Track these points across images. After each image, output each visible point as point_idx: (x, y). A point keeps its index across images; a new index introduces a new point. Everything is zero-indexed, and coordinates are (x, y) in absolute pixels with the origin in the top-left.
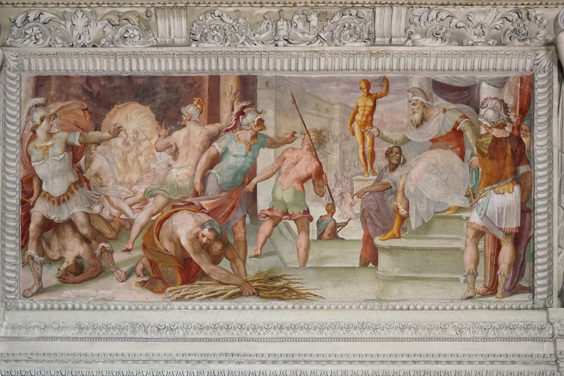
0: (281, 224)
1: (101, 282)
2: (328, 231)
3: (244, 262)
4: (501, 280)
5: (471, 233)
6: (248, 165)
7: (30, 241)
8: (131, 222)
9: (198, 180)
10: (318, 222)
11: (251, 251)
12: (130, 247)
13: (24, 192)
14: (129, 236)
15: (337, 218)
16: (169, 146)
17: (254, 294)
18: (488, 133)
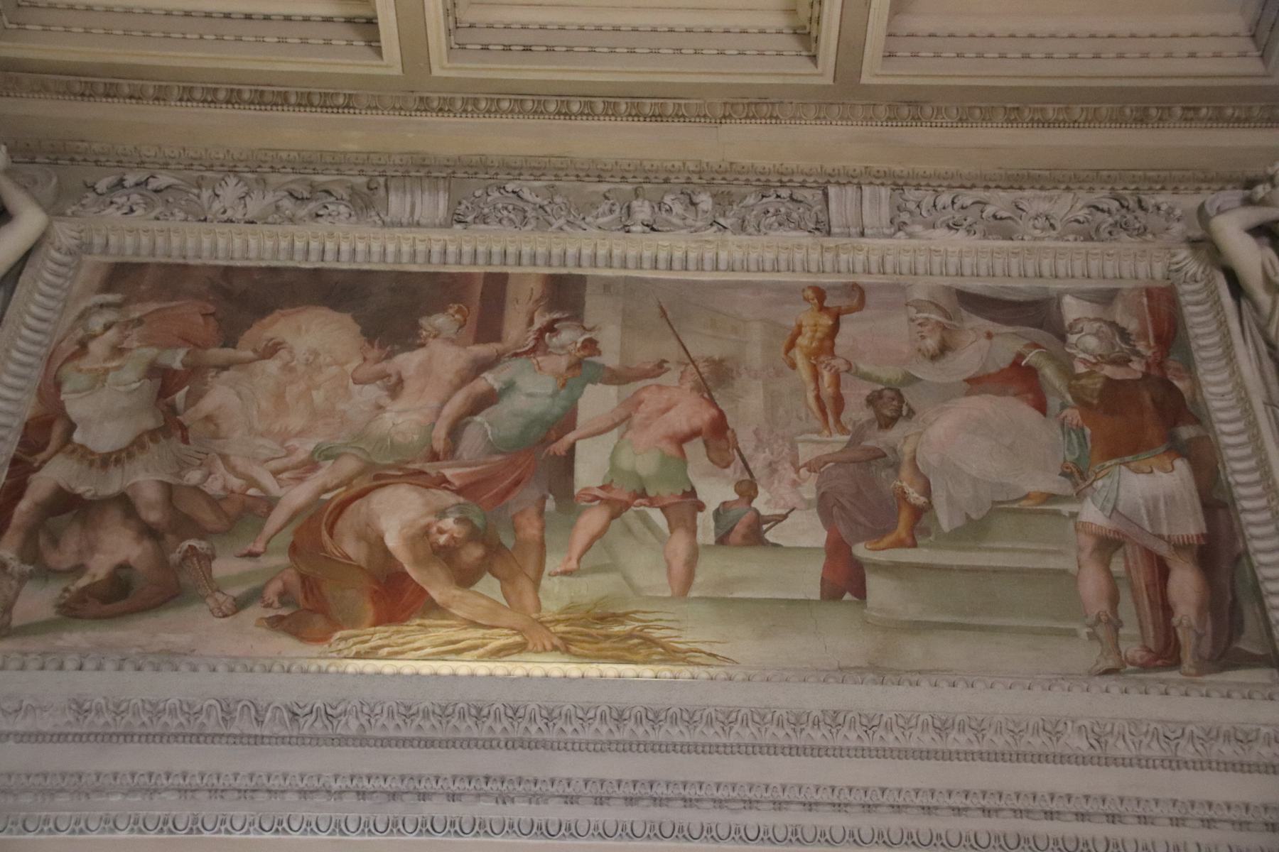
0: (629, 515)
1: (169, 616)
2: (740, 529)
3: (536, 583)
4: (1186, 639)
5: (1088, 543)
6: (557, 410)
7: (9, 532)
8: (271, 503)
9: (441, 432)
10: (717, 514)
11: (554, 562)
12: (259, 547)
13: (23, 443)
14: (260, 528)
15: (762, 504)
16: (383, 376)
17: (555, 648)
18: (1090, 374)
